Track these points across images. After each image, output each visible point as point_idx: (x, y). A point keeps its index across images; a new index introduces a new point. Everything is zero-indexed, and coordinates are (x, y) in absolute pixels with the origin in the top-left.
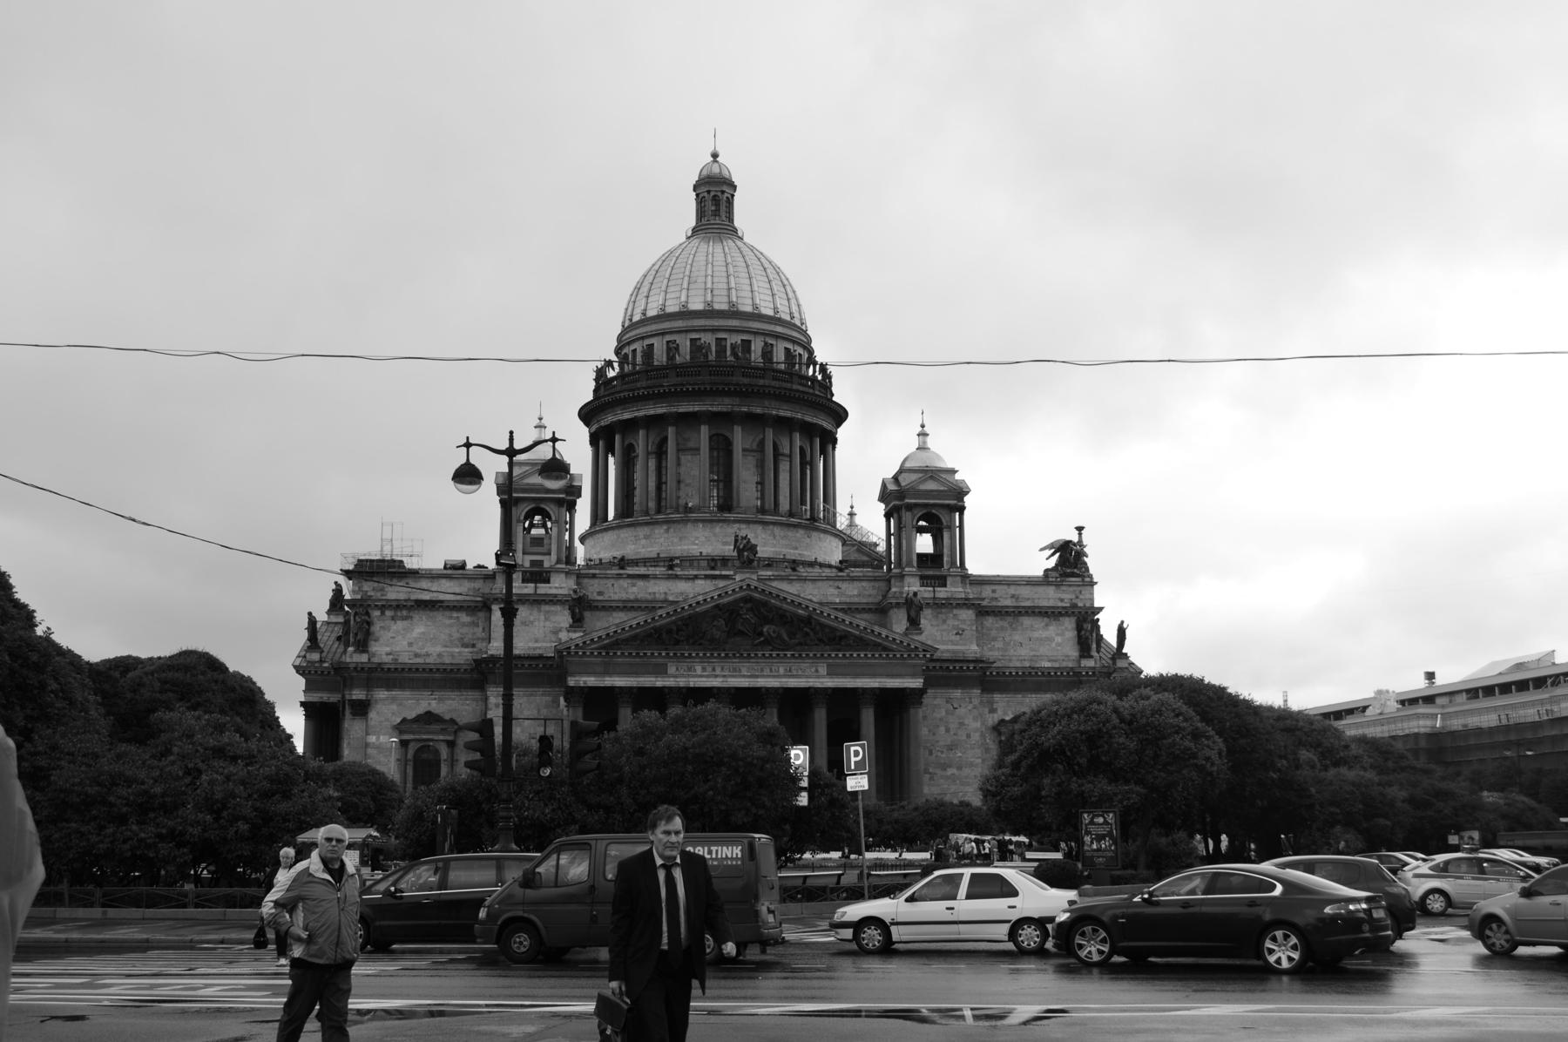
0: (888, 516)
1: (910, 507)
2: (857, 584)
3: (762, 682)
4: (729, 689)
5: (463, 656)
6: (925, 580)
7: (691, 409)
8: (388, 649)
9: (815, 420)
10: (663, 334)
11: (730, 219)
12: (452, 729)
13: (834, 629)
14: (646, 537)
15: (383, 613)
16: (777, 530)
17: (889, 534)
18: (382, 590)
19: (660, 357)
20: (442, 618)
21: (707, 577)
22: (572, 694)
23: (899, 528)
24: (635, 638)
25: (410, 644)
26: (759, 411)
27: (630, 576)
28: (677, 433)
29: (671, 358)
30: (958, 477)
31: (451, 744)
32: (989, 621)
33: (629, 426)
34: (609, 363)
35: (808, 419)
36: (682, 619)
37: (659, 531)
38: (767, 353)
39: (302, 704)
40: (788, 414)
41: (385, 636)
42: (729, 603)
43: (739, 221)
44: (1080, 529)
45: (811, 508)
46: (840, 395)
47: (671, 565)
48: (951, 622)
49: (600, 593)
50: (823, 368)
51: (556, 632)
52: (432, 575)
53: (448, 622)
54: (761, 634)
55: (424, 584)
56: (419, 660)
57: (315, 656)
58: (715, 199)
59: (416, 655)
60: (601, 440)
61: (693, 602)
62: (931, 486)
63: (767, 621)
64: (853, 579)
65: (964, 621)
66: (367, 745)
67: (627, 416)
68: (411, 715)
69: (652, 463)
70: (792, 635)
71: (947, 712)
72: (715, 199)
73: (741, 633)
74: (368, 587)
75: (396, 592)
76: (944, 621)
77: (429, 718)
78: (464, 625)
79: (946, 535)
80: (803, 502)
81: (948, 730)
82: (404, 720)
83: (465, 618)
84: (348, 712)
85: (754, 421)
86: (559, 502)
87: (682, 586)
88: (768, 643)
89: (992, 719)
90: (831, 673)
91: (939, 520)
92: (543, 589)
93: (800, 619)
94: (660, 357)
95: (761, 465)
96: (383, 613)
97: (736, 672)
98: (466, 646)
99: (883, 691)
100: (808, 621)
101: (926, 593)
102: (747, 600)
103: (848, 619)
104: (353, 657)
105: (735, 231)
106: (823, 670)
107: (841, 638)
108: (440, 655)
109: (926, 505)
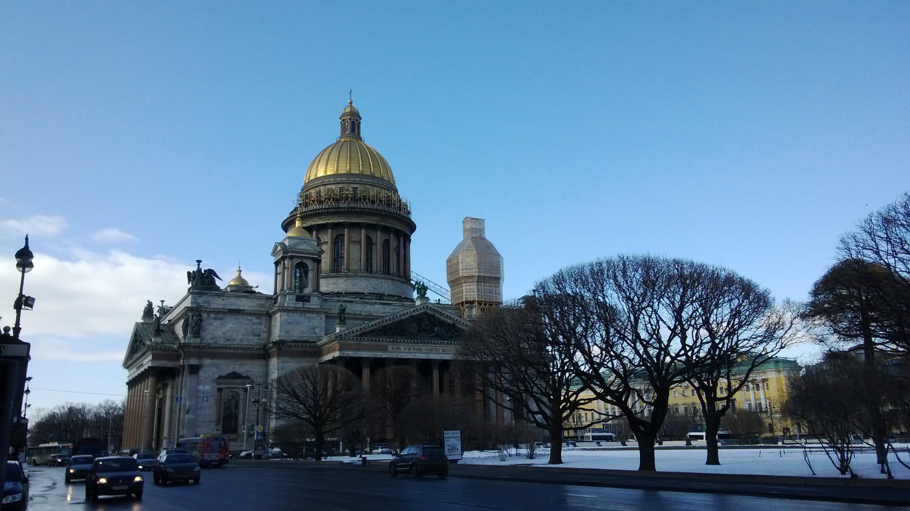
3: (432, 356)
5: (254, 341)
11: (359, 133)
14: (333, 284)
15: (209, 315)
16: (398, 284)
18: (208, 302)
20: (243, 319)
21: (381, 304)
24: (373, 331)
25: (224, 334)
28: (349, 232)
37: (341, 281)
43: (362, 135)
51: (313, 329)
53: (245, 322)
54: (434, 332)
55: (233, 300)
56: (229, 343)
58: (352, 123)
59: (228, 340)
61: (401, 313)
63: (434, 325)
66: (198, 391)
67: (321, 222)
68: (224, 374)
72: (352, 123)
73: (424, 330)
74: (200, 300)
77: (234, 375)
78: (254, 324)
82: (220, 377)
83: (255, 320)
85: (386, 230)
86: (313, 259)
87: (369, 308)
88: (437, 336)
92: (307, 305)
93: (449, 325)
96: (209, 315)
98: (255, 335)
100: (454, 326)
102: (426, 314)
104: (190, 340)
105: (361, 139)
108: (241, 340)
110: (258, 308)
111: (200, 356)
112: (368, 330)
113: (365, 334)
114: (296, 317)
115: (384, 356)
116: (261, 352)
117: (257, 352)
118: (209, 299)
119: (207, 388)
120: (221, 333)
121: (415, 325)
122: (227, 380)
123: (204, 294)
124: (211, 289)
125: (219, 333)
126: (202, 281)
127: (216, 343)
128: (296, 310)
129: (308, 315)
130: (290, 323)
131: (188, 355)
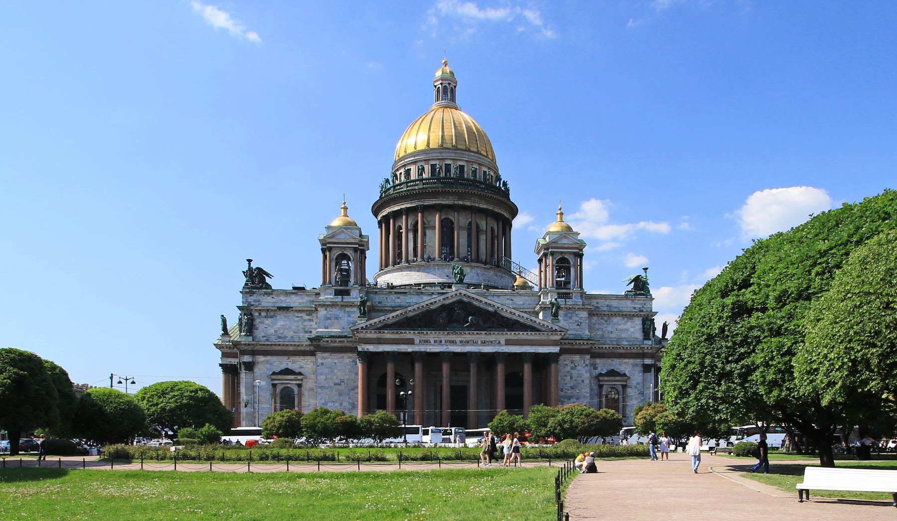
0: (540, 261)
1: (552, 254)
2: (523, 298)
4: (449, 353)
6: (560, 295)
7: (431, 203)
8: (263, 334)
9: (500, 211)
10: (414, 163)
12: (300, 377)
13: (509, 319)
15: (260, 314)
17: (541, 271)
19: (414, 176)
22: (359, 353)
23: (546, 266)
25: (276, 331)
26: (468, 204)
27: (396, 293)
29: (420, 174)
30: (579, 237)
31: (300, 386)
32: (595, 318)
33: (396, 215)
34: (387, 181)
35: (496, 210)
36: (422, 313)
38: (474, 172)
39: (221, 365)
40: (485, 206)
41: (261, 327)
42: (450, 304)
44: (645, 269)
45: (498, 258)
46: (514, 197)
47: (418, 289)
48: (574, 318)
49: (380, 303)
50: (505, 184)
52: (286, 293)
55: (282, 298)
57: (227, 339)
59: (280, 337)
60: (384, 222)
62: (565, 241)
64: (520, 295)
65: (581, 318)
66: (254, 386)
67: (396, 208)
68: (278, 370)
69: (411, 236)
70: (485, 322)
71: (572, 368)
74: (251, 299)
75: (267, 302)
76: (571, 318)
77: (287, 372)
79: (572, 270)
80: (492, 255)
81: (571, 378)
82: (274, 373)
84: (243, 368)
89: (597, 372)
90: (508, 343)
91: (569, 262)
92: (347, 299)
94: (414, 176)
95: (469, 236)
96: (260, 314)
97: (453, 342)
98: (306, 332)
99: (537, 355)
101: (561, 302)
102: (460, 302)
103: (517, 313)
106: (503, 342)
107: (513, 324)
109: (562, 253)
110: (308, 304)
111: (254, 353)
112: (390, 322)
113: (386, 327)
114: (335, 311)
115: (410, 350)
116: (312, 348)
117: (308, 349)
118: (261, 298)
119: (263, 383)
120: (273, 331)
121: (444, 314)
122: (280, 377)
123: (254, 293)
124: (261, 288)
125: (271, 331)
126: (256, 279)
127: (267, 340)
128: (334, 305)
129: (348, 309)
130: (329, 318)
131: (244, 353)
